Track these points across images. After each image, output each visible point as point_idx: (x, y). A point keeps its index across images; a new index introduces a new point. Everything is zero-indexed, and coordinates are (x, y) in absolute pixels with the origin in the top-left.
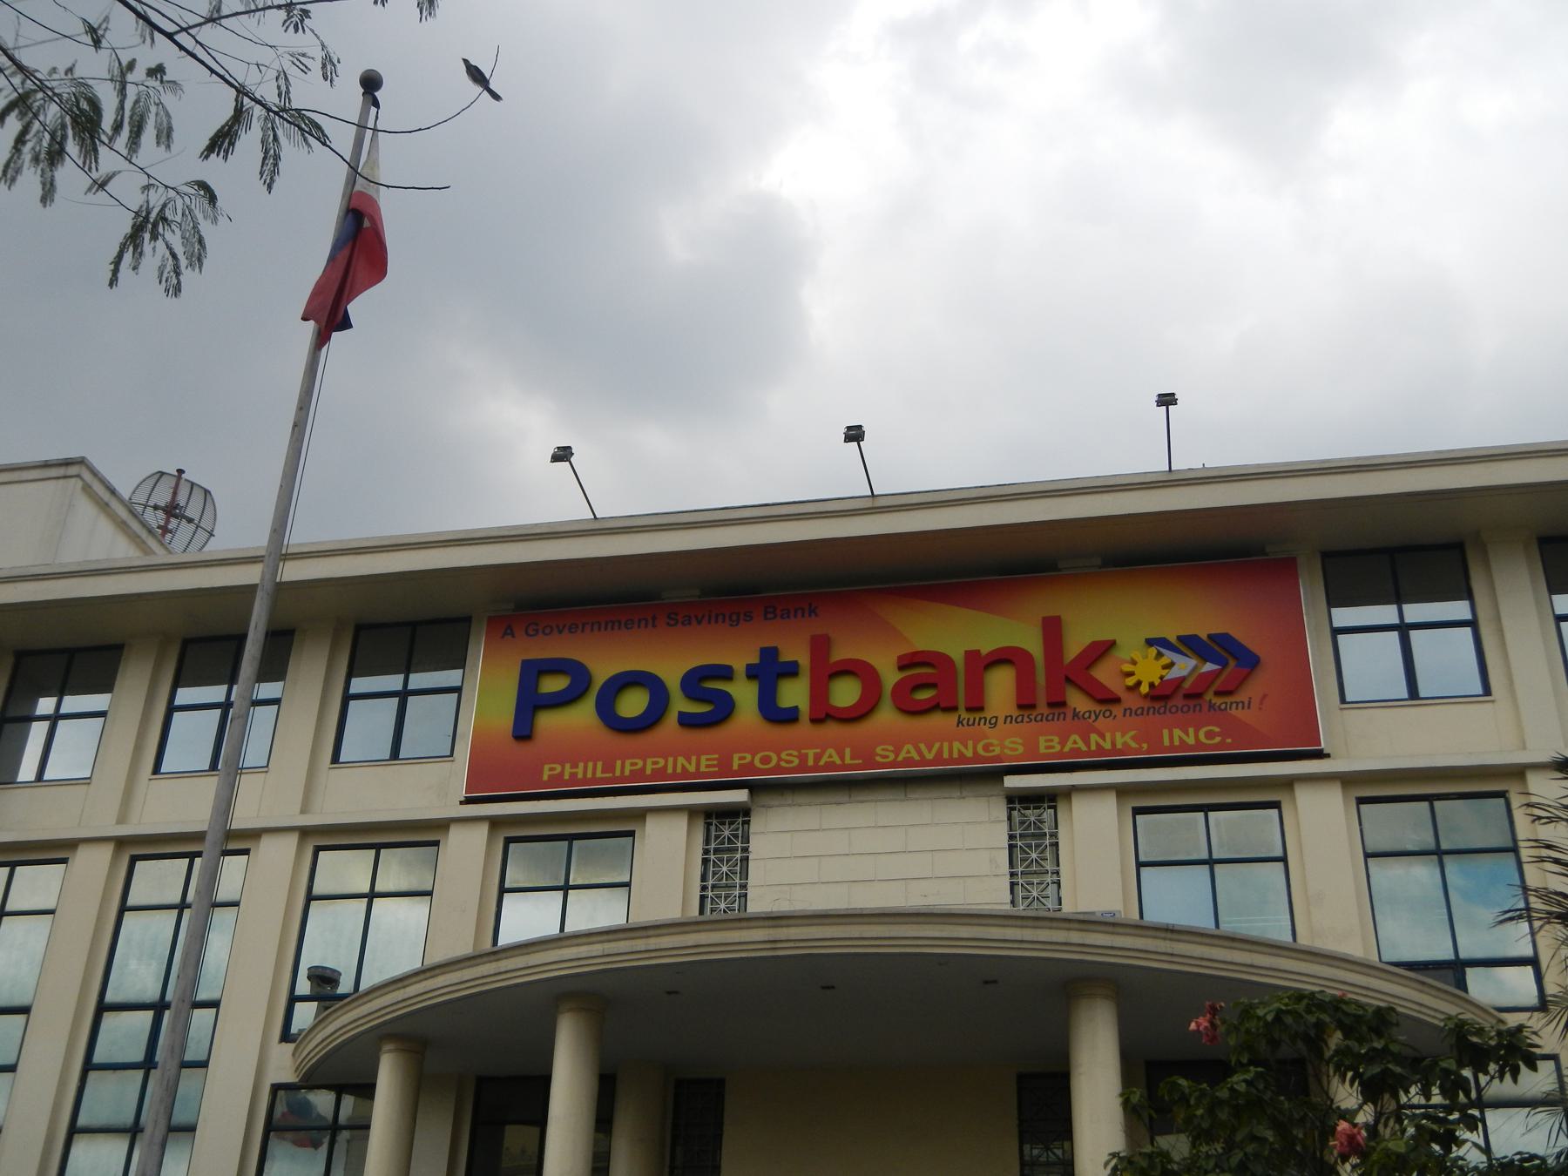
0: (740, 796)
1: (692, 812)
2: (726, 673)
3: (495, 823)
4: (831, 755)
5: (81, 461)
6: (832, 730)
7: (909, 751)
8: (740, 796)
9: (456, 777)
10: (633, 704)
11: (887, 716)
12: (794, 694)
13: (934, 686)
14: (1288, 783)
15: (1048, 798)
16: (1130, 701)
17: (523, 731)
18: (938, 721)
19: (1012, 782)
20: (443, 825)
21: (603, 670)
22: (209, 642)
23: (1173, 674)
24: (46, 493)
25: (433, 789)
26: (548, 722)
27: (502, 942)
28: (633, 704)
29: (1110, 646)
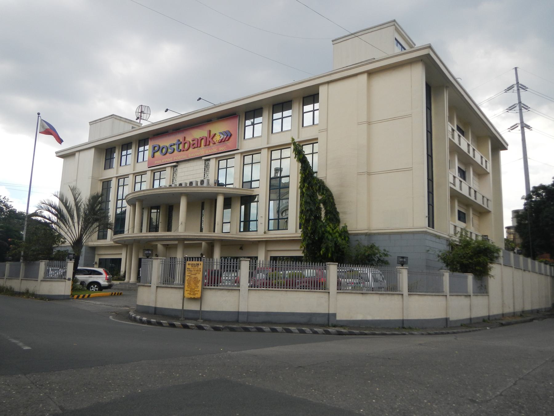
0: (175, 164)
1: (171, 166)
2: (174, 144)
3: (152, 170)
4: (184, 157)
5: (113, 115)
6: (185, 152)
7: (192, 155)
8: (175, 164)
9: (146, 164)
10: (164, 150)
11: (191, 149)
12: (181, 147)
13: (197, 144)
14: (234, 154)
15: (209, 160)
16: (217, 143)
17: (153, 157)
18: (196, 149)
19: (203, 158)
20: (146, 171)
21: (161, 145)
22: (126, 144)
23: (222, 138)
24: (110, 121)
25: (142, 167)
26: (156, 154)
27: (155, 187)
28: (164, 150)
29: (215, 134)
